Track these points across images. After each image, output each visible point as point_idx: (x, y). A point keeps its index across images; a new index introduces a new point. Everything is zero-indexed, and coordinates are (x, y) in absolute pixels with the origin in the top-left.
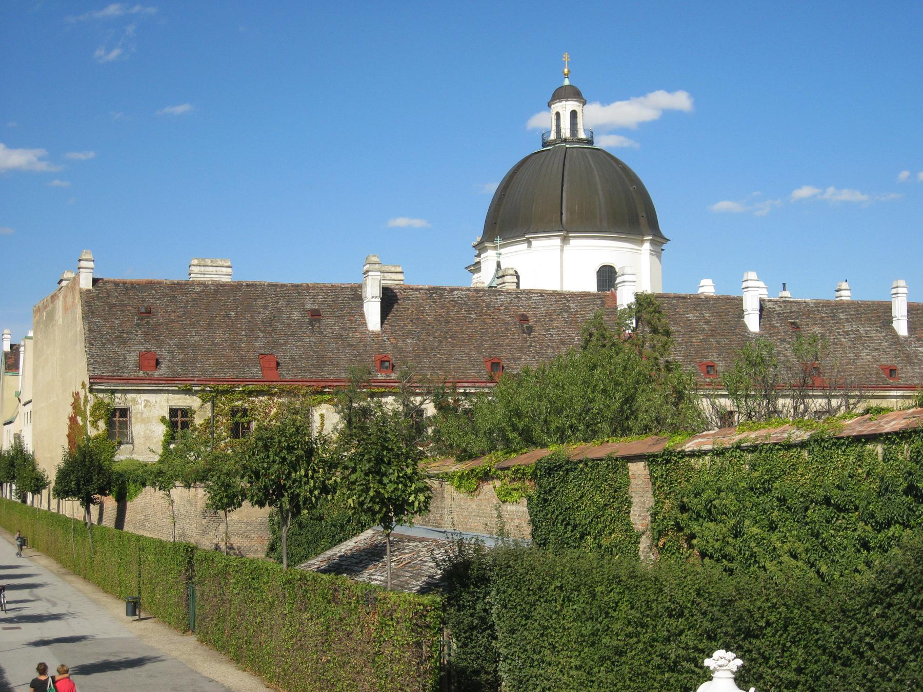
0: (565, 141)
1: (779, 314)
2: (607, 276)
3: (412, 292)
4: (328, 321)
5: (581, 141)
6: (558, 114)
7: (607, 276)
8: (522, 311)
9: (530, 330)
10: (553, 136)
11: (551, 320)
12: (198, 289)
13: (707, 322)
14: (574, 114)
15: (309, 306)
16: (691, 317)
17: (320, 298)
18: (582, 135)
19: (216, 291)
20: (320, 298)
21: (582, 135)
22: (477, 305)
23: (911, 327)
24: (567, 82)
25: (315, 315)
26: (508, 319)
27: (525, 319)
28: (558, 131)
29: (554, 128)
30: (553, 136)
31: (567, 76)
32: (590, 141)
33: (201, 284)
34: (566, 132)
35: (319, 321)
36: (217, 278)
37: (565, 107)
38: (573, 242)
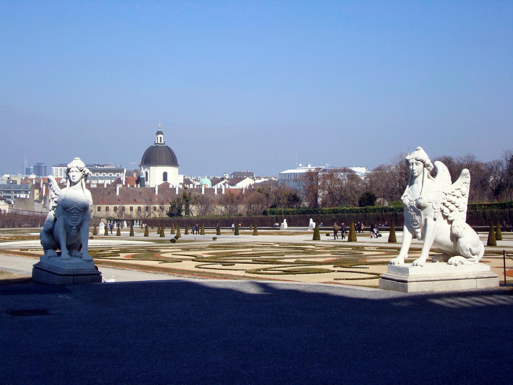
1: (182, 191)
2: (165, 175)
3: (124, 189)
4: (111, 193)
6: (157, 137)
7: (165, 175)
8: (140, 191)
9: (141, 194)
11: (145, 193)
12: (92, 189)
13: (170, 192)
14: (161, 138)
15: (108, 191)
17: (110, 190)
18: (163, 142)
19: (95, 189)
20: (110, 190)
21: (163, 142)
22: (133, 190)
24: (160, 130)
25: (109, 192)
26: (138, 192)
27: (140, 192)
28: (157, 142)
29: (157, 140)
30: (156, 142)
31: (160, 128)
32: (163, 144)
33: (92, 188)
34: (159, 142)
35: (110, 193)
36: (94, 187)
38: (157, 167)
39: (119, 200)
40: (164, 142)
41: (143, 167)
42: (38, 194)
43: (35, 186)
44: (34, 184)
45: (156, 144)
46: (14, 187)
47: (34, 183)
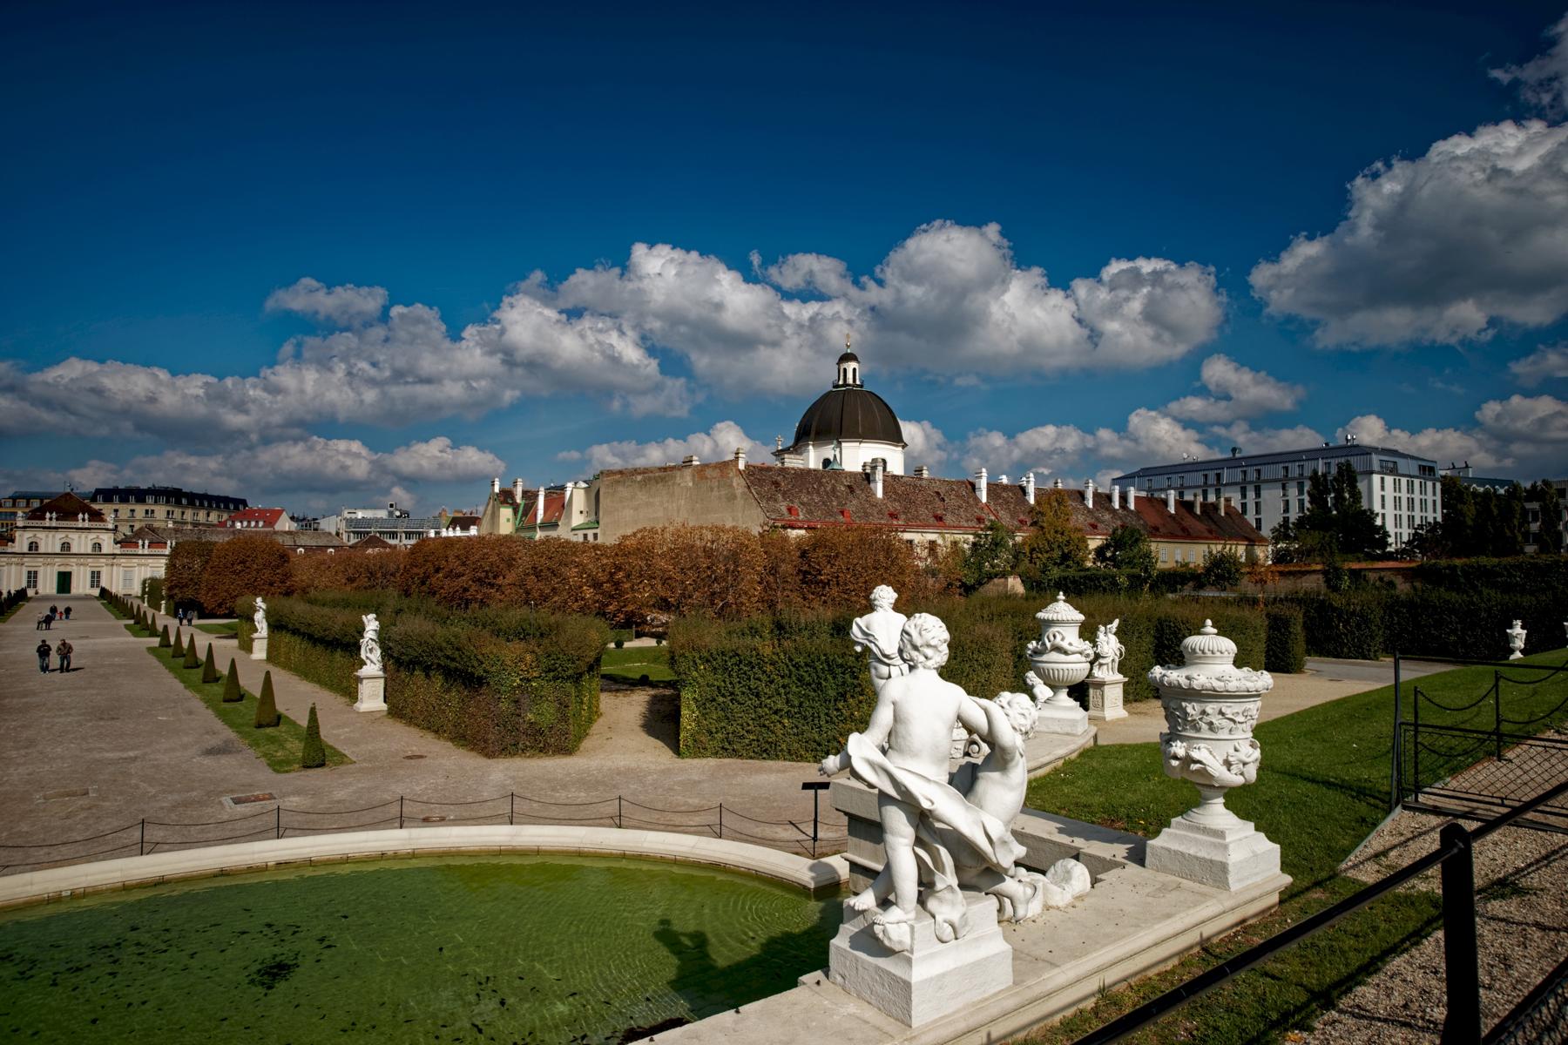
0: (849, 385)
5: (858, 386)
6: (845, 370)
9: (943, 500)
10: (841, 382)
14: (854, 370)
16: (1004, 495)
18: (858, 382)
21: (858, 382)
23: (1094, 503)
24: (849, 351)
25: (850, 487)
27: (938, 493)
29: (842, 377)
32: (861, 386)
33: (793, 469)
34: (850, 381)
37: (851, 366)
38: (863, 445)
39: (893, 516)
40: (862, 382)
41: (813, 445)
42: (508, 520)
43: (502, 499)
44: (497, 494)
45: (836, 386)
46: (405, 525)
47: (497, 490)
